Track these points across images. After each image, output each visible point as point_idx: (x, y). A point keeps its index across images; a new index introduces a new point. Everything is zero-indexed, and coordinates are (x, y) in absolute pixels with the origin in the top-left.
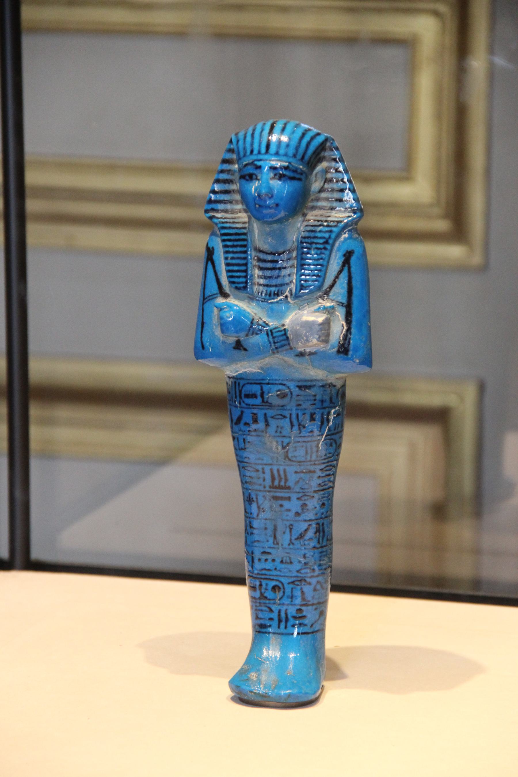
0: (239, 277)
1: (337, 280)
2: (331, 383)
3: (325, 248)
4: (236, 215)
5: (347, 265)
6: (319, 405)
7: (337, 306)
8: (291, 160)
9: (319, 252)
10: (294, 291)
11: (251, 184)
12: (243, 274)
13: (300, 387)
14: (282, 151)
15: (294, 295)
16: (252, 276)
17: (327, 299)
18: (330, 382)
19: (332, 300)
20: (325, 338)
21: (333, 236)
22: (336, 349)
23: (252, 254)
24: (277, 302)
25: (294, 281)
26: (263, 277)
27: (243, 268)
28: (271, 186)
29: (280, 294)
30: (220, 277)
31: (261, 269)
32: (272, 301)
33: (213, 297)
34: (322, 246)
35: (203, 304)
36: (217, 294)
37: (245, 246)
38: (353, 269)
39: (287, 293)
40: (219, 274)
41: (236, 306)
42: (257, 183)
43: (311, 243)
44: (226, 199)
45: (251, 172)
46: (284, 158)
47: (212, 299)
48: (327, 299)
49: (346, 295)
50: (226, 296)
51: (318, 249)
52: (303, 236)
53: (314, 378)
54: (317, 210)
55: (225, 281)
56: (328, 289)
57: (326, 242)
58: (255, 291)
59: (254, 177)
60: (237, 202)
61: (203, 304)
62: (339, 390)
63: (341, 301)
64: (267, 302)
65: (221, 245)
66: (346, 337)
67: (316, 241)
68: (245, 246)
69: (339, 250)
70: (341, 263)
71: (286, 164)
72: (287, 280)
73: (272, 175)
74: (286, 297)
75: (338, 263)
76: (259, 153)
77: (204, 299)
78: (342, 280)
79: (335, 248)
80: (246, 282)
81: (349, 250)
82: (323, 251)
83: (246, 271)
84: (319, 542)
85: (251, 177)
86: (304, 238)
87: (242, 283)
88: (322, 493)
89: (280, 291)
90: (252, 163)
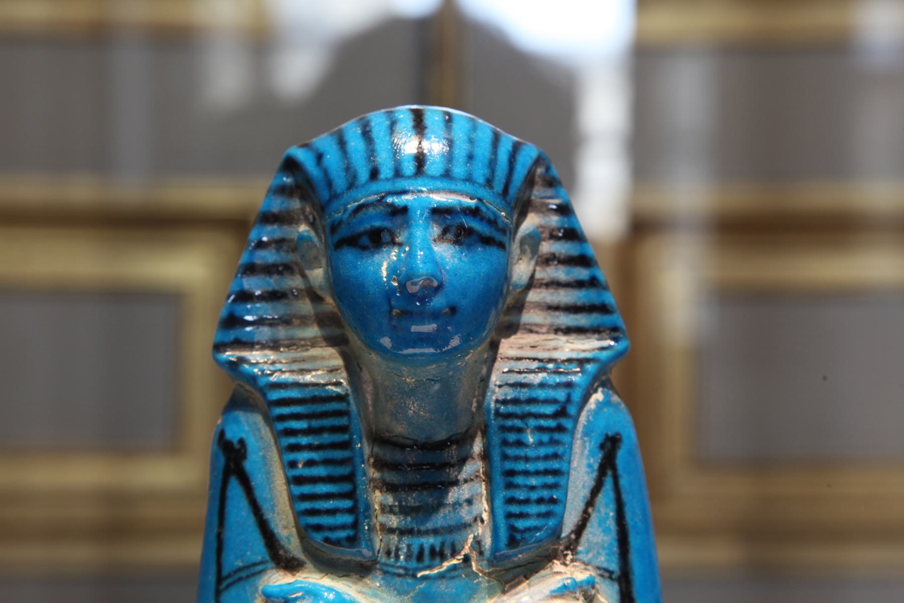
0: (332, 512)
1: (590, 510)
3: (560, 429)
4: (305, 354)
5: (609, 473)
7: (598, 579)
8: (483, 193)
9: (545, 438)
10: (488, 542)
11: (377, 258)
12: (347, 504)
14: (459, 170)
15: (487, 554)
16: (368, 507)
17: (572, 561)
19: (586, 564)
21: (577, 395)
24: (441, 576)
25: (485, 516)
26: (397, 509)
27: (346, 487)
28: (439, 260)
29: (448, 552)
30: (268, 515)
31: (391, 488)
32: (427, 573)
33: (251, 572)
34: (551, 423)
35: (218, 593)
36: (262, 562)
37: (343, 429)
38: (623, 482)
39: (466, 550)
40: (265, 507)
41: (330, 590)
42: (394, 254)
43: (524, 417)
45: (377, 224)
46: (468, 187)
47: (248, 577)
48: (572, 561)
49: (615, 549)
50: (291, 565)
51: (541, 429)
52: (501, 398)
54: (519, 335)
55: (285, 527)
56: (573, 536)
57: (562, 413)
58: (377, 547)
59: (386, 237)
60: (304, 321)
61: (218, 593)
63: (605, 565)
64: (414, 576)
65: (266, 432)
67: (534, 409)
68: (343, 429)
69: (587, 433)
70: (596, 466)
71: (472, 203)
72: (465, 514)
73: (436, 230)
74: (467, 559)
75: (589, 466)
76: (398, 173)
77: (220, 579)
78: (603, 510)
79: (580, 428)
80: (355, 525)
81: (610, 434)
82: (557, 436)
83: (351, 495)
85: (377, 240)
86: (505, 402)
87: (343, 527)
89: (448, 544)
90: (381, 200)
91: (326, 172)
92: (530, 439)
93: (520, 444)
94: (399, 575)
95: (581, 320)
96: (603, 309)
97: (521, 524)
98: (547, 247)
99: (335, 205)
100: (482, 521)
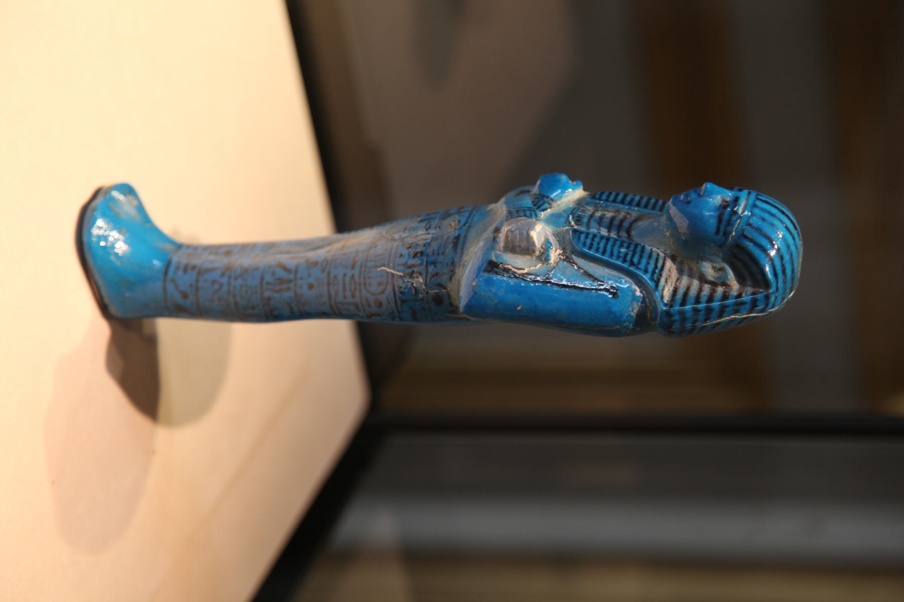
2: (455, 273)
6: (431, 259)
9: (622, 255)
13: (458, 238)
18: (457, 271)
20: (511, 248)
22: (494, 259)
23: (635, 212)
51: (626, 254)
53: (466, 252)
57: (632, 263)
62: (445, 288)
66: (507, 270)
84: (268, 283)
88: (326, 281)
92: (623, 250)
93: (621, 246)
95: (679, 296)
96: (683, 303)
97: (583, 236)
98: (720, 290)
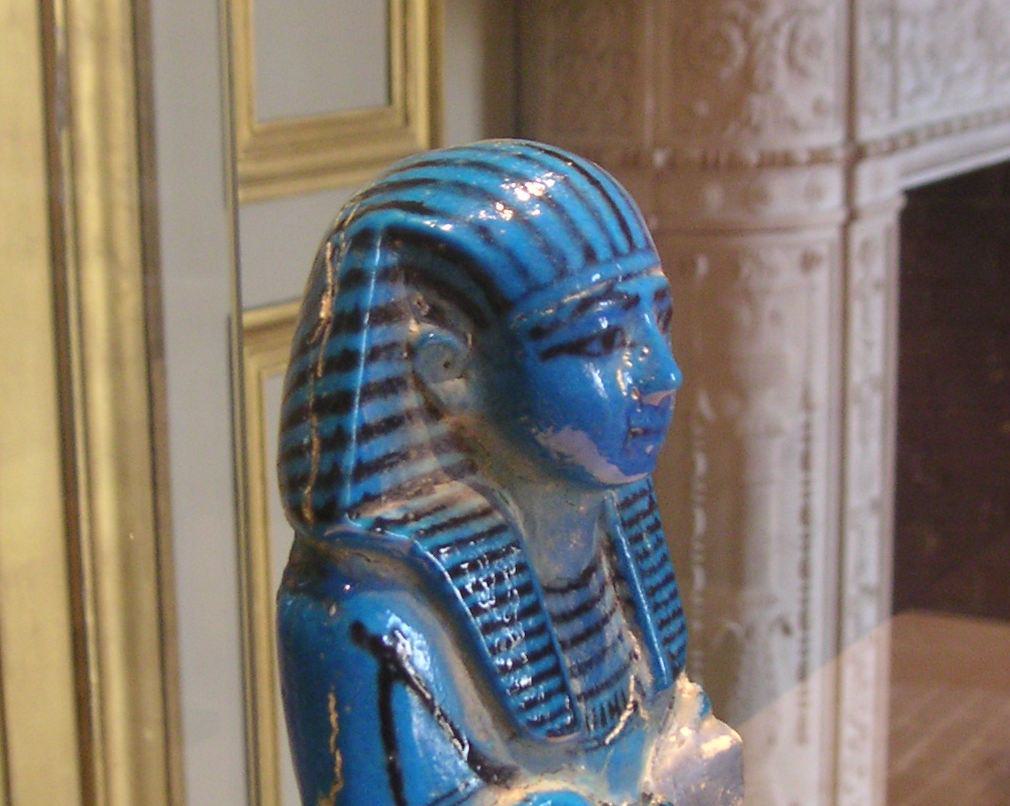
32: (612, 736)
44: (392, 451)
64: (604, 744)
76: (616, 253)
91: (510, 253)
94: (596, 748)
99: (537, 300)
100: (636, 657)
